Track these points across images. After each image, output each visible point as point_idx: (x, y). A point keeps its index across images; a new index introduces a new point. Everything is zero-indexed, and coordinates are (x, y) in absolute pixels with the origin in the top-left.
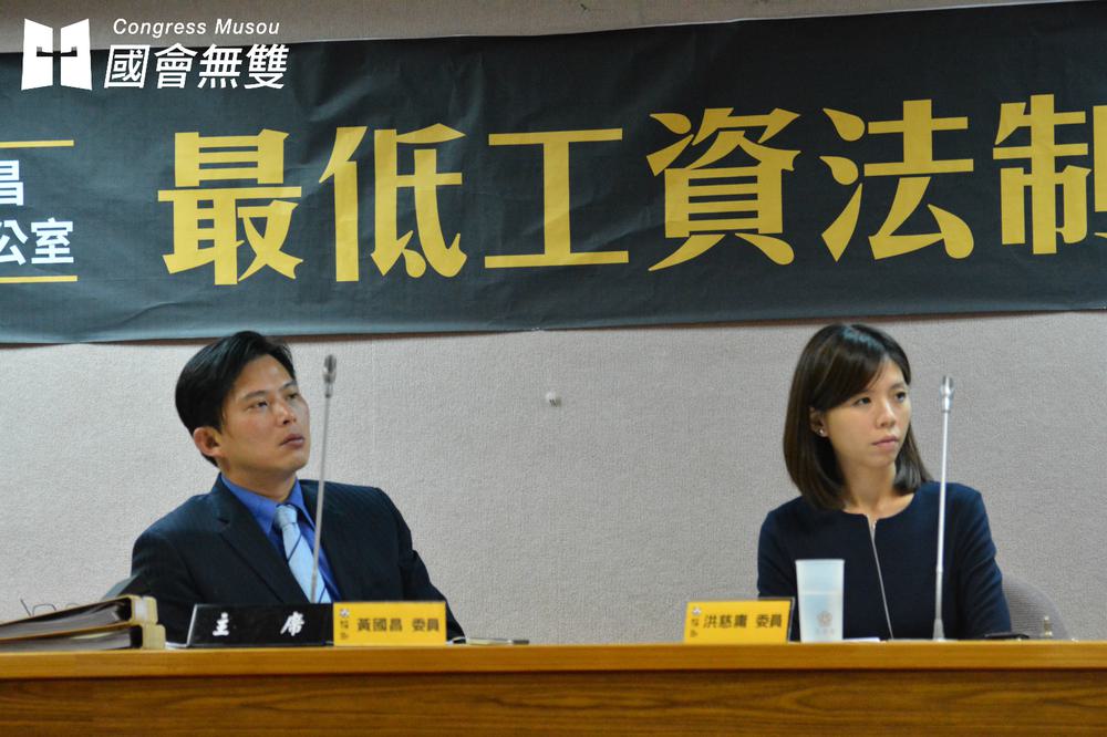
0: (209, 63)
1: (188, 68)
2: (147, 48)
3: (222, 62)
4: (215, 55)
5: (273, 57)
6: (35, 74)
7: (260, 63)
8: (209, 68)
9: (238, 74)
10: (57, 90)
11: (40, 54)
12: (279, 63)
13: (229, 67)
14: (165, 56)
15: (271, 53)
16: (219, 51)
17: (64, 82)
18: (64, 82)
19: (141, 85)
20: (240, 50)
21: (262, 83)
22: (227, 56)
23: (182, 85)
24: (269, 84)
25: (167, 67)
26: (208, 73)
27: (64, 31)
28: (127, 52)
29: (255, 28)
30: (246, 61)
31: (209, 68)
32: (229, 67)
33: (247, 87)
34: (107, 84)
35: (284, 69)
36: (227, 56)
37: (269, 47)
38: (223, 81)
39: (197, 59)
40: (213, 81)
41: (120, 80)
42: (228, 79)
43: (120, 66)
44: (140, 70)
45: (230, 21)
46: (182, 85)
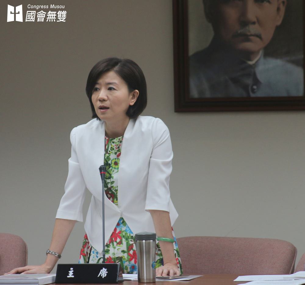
0: (49, 15)
1: (44, 17)
2: (35, 12)
3: (52, 15)
4: (50, 13)
5: (63, 14)
6: (10, 18)
7: (60, 15)
8: (49, 17)
9: (55, 18)
10: (15, 22)
11: (11, 13)
12: (65, 15)
13: (53, 16)
14: (39, 14)
15: (63, 13)
16: (51, 12)
17: (16, 20)
18: (16, 20)
19: (34, 21)
20: (56, 12)
21: (61, 20)
22: (53, 14)
23: (43, 21)
24: (62, 20)
25: (40, 17)
26: (49, 18)
27: (17, 7)
28: (31, 13)
29: (59, 7)
30: (57, 15)
31: (49, 17)
32: (53, 16)
33: (57, 21)
34: (26, 21)
35: (66, 17)
36: (53, 14)
37: (62, 11)
38: (52, 20)
39: (46, 14)
40: (50, 20)
41: (29, 20)
42: (53, 19)
43: (29, 16)
44: (33, 17)
45: (54, 5)
46: (43, 21)
